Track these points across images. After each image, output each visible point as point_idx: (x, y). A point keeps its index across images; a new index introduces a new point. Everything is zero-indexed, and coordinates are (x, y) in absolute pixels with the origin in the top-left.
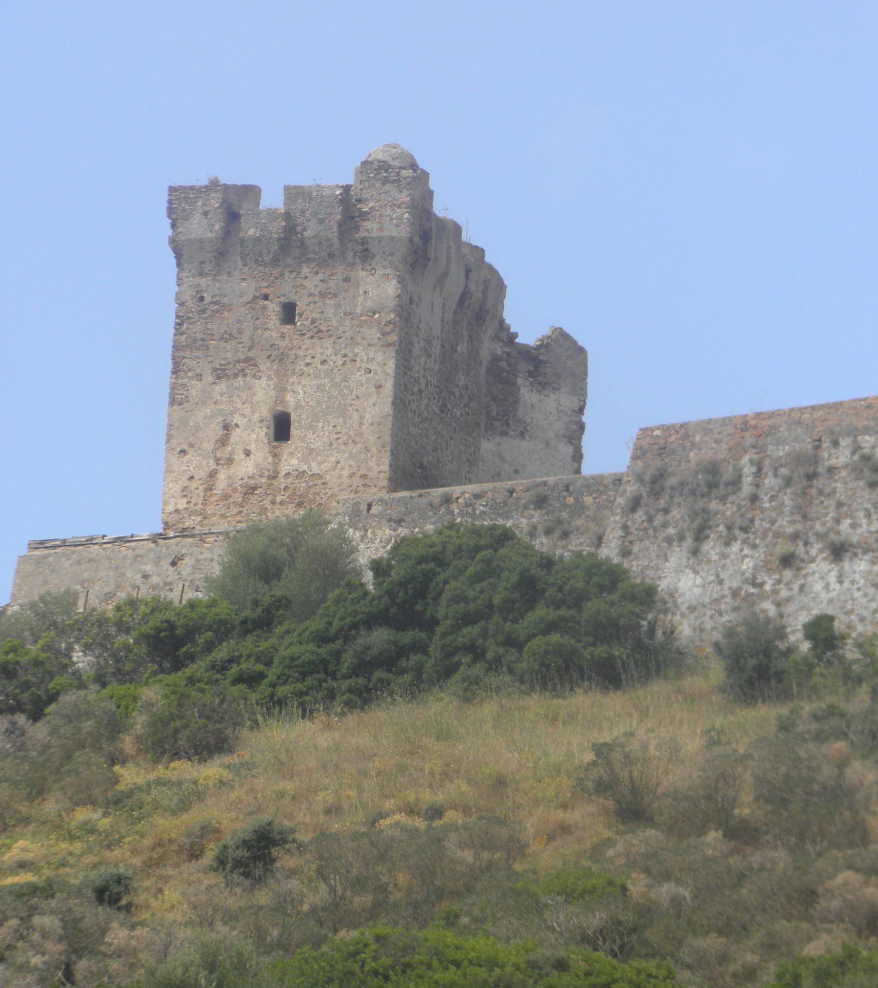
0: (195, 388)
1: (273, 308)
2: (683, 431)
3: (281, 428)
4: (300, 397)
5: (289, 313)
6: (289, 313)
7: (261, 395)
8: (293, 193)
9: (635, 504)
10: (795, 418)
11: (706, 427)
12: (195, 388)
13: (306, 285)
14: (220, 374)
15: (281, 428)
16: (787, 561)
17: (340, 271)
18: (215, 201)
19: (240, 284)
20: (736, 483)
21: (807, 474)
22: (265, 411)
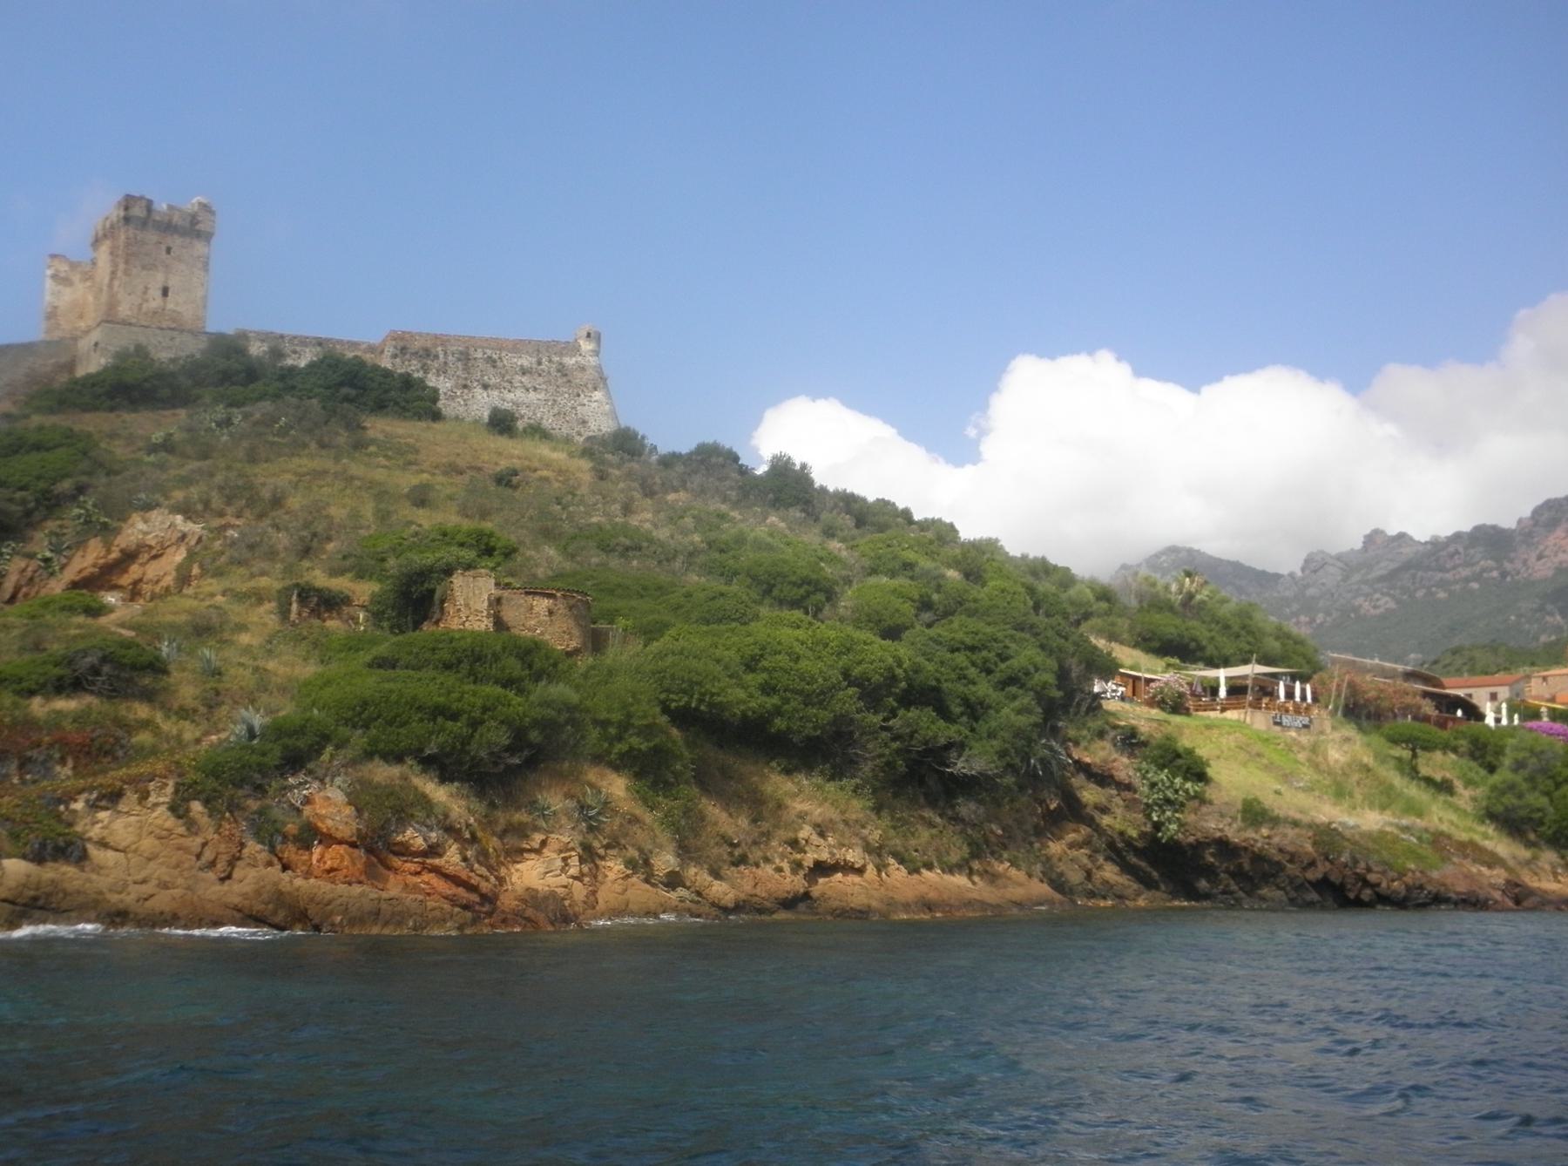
0: (135, 271)
1: (163, 247)
2: (412, 335)
3: (165, 292)
4: (173, 282)
5: (169, 250)
6: (169, 250)
7: (159, 278)
8: (170, 207)
9: (395, 356)
10: (458, 339)
11: (420, 335)
12: (135, 271)
13: (176, 241)
14: (144, 267)
15: (165, 292)
16: (465, 386)
17: (188, 240)
18: (144, 203)
19: (151, 236)
20: (436, 357)
21: (465, 358)
22: (160, 285)
